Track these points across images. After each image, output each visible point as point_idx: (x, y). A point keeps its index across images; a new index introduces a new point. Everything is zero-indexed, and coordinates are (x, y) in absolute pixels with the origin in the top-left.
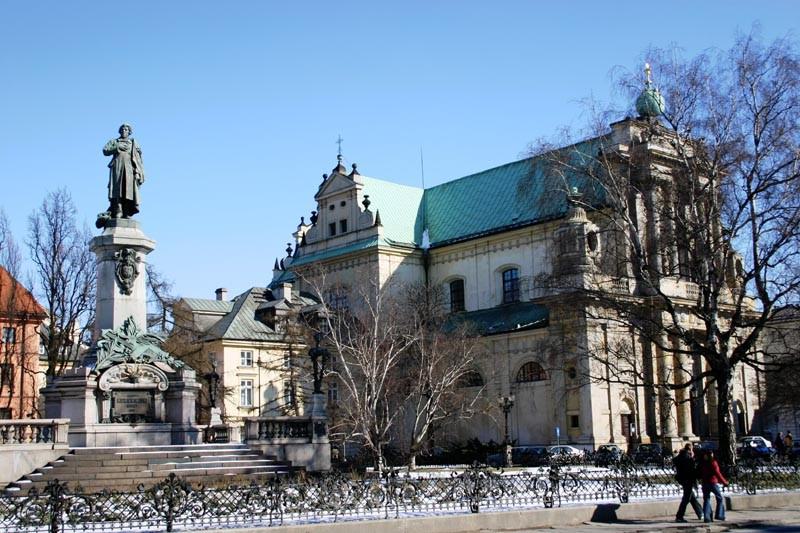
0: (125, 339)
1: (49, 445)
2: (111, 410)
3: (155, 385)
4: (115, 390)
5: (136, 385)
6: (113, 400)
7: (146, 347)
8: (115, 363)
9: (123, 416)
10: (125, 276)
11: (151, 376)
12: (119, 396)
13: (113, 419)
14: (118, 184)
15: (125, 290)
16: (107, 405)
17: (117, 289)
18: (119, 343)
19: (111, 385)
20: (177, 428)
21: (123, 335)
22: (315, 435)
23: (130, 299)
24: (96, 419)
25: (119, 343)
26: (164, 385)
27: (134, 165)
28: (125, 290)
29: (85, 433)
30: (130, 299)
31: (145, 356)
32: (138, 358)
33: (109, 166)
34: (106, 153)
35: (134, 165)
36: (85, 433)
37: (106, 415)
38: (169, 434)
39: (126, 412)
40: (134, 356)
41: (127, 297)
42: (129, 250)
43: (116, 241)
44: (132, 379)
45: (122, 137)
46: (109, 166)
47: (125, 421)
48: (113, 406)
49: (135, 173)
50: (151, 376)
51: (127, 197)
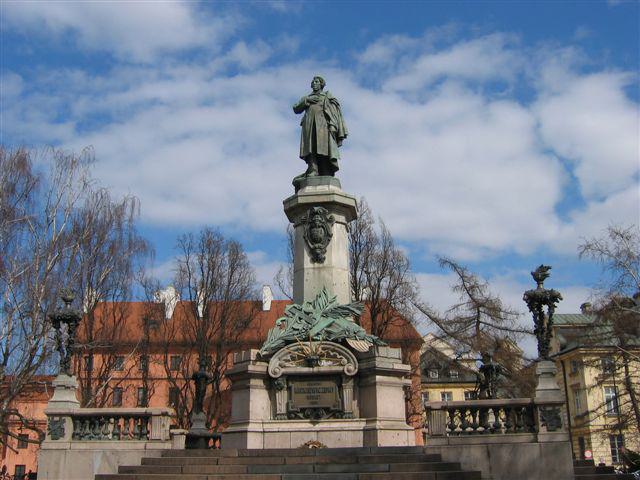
0: (308, 314)
1: (141, 444)
2: (287, 404)
3: (341, 368)
5: (316, 369)
6: (289, 389)
7: (330, 320)
8: (287, 342)
9: (303, 410)
10: (315, 240)
11: (335, 356)
12: (294, 385)
13: (291, 415)
14: (309, 135)
16: (282, 397)
17: (307, 258)
18: (300, 319)
19: (283, 370)
21: (311, 308)
22: (543, 430)
23: (324, 267)
24: (268, 416)
25: (300, 319)
26: (352, 368)
27: (327, 118)
28: (317, 258)
29: (246, 432)
30: (324, 267)
31: (327, 332)
32: (318, 334)
35: (327, 118)
36: (246, 432)
37: (282, 409)
38: (362, 433)
39: (306, 404)
40: (312, 333)
41: (321, 265)
42: (316, 208)
43: (301, 200)
44: (309, 362)
45: (315, 91)
47: (307, 417)
48: (290, 397)
49: (329, 126)
50: (335, 356)
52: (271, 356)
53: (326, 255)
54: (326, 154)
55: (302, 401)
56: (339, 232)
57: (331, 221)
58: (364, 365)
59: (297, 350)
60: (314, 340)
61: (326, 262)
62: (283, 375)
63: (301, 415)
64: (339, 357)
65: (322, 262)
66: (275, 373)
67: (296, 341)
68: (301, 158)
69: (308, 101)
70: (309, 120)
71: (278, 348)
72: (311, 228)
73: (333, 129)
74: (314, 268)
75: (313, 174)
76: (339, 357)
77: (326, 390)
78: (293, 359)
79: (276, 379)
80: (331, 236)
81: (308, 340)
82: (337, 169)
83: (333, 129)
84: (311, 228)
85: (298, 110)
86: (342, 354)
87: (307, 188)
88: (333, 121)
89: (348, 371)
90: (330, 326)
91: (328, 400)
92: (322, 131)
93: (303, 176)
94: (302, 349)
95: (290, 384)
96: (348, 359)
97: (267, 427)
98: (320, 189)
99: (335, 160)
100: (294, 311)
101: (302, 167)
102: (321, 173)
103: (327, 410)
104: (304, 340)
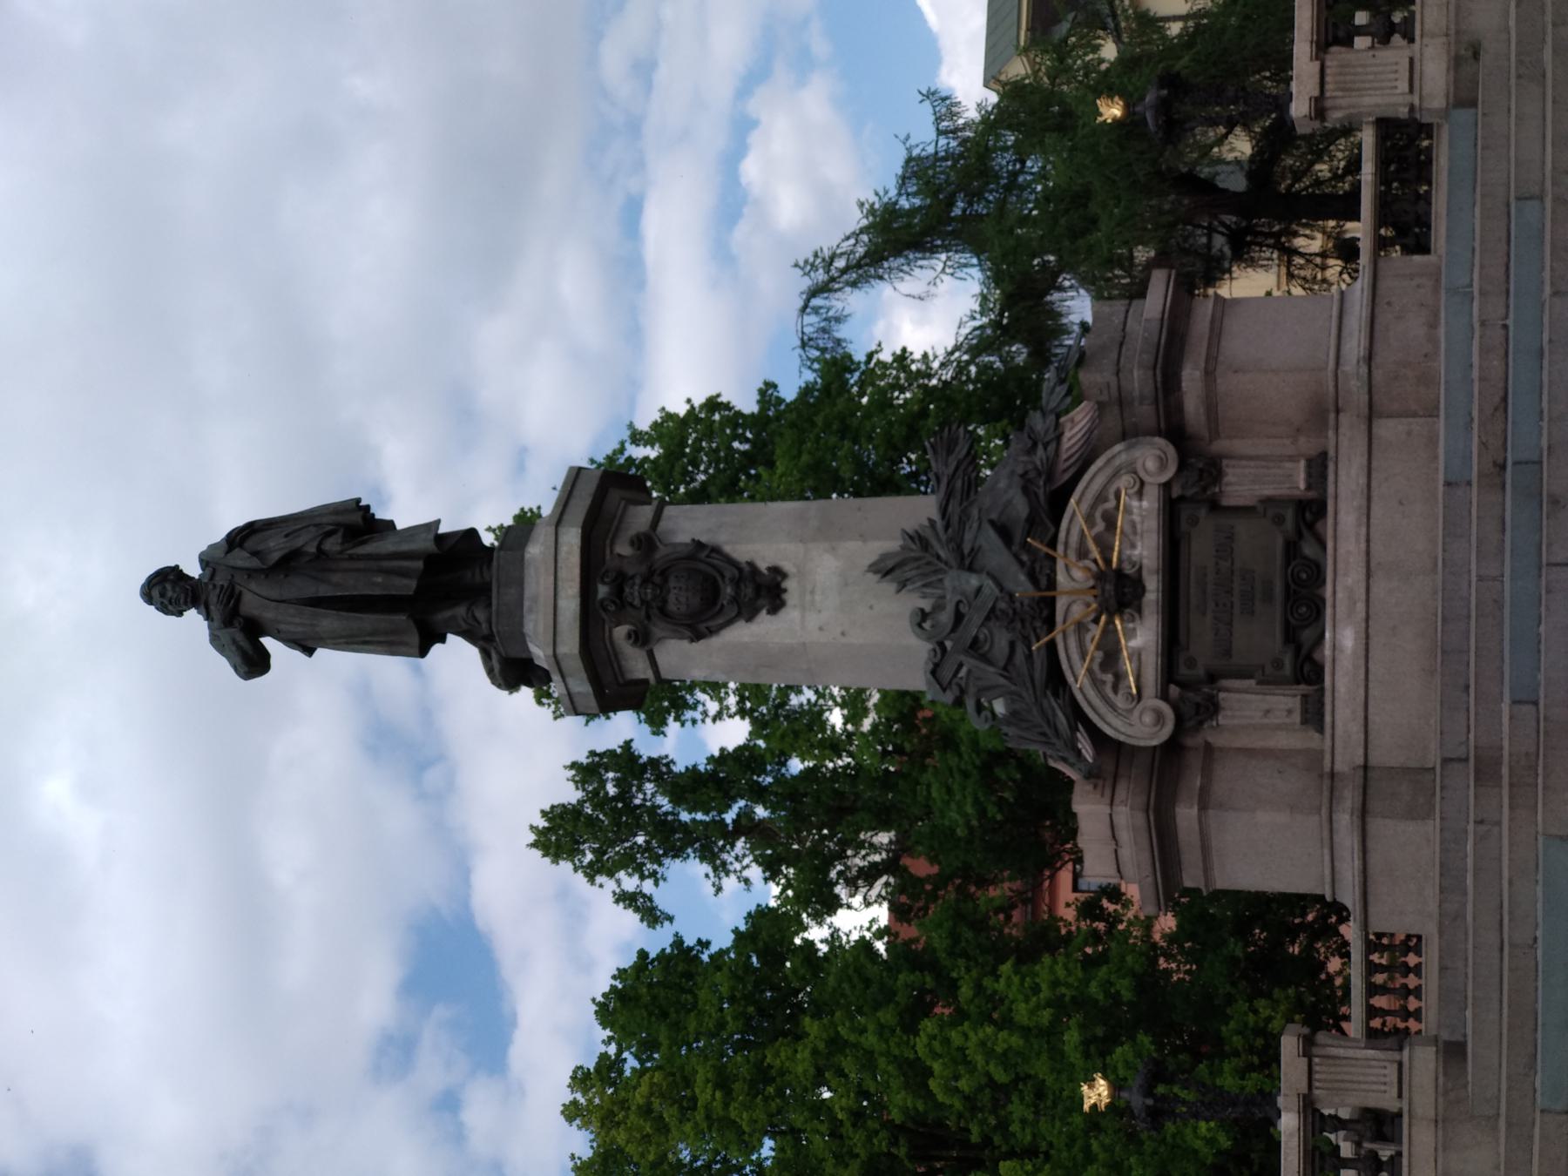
0: (959, 617)
4: (1169, 673)
5: (1153, 587)
6: (1212, 678)
8: (1056, 679)
9: (1290, 636)
13: (1306, 670)
15: (765, 590)
20: (1355, 388)
27: (289, 563)
28: (765, 590)
32: (1033, 578)
33: (309, 651)
34: (254, 663)
37: (1286, 702)
42: (603, 591)
43: (570, 644)
46: (309, 651)
51: (408, 586)
52: (1096, 736)
53: (763, 566)
54: (420, 564)
55: (1260, 634)
56: (688, 524)
57: (646, 542)
58: (1145, 412)
59: (1083, 656)
60: (1052, 584)
61: (787, 566)
62: (1164, 696)
63: (1307, 635)
64: (1111, 504)
65: (784, 576)
66: (1159, 718)
67: (1052, 647)
68: (423, 652)
69: (228, 622)
70: (297, 620)
71: (1077, 715)
72: (664, 614)
73: (332, 545)
74: (803, 608)
75: (481, 615)
76: (1111, 504)
77: (1226, 546)
78: (1110, 657)
79: (1179, 720)
80: (699, 545)
81: (1051, 603)
82: (472, 534)
83: (332, 545)
84: (664, 614)
85: (254, 663)
86: (1105, 488)
87: (529, 627)
88: (306, 541)
89: (1163, 465)
90: (1004, 532)
91: (1258, 548)
92: (336, 578)
93: (486, 655)
94: (1081, 627)
95: (1200, 671)
96: (1116, 475)
97: (1347, 757)
98: (537, 583)
99: (441, 539)
100: (946, 674)
101: (457, 658)
102: (481, 593)
103: (1291, 549)
104: (1050, 623)
